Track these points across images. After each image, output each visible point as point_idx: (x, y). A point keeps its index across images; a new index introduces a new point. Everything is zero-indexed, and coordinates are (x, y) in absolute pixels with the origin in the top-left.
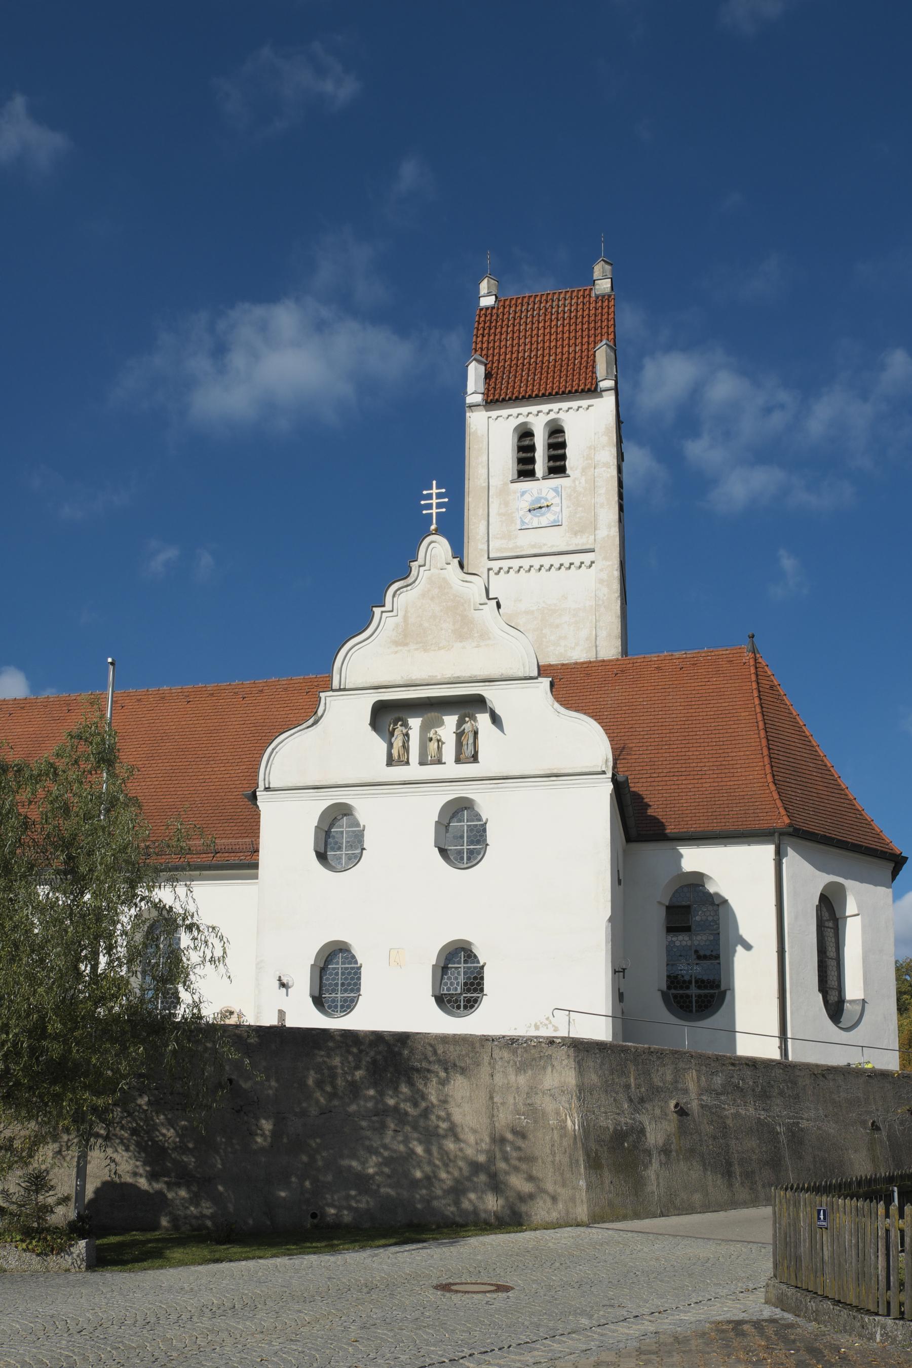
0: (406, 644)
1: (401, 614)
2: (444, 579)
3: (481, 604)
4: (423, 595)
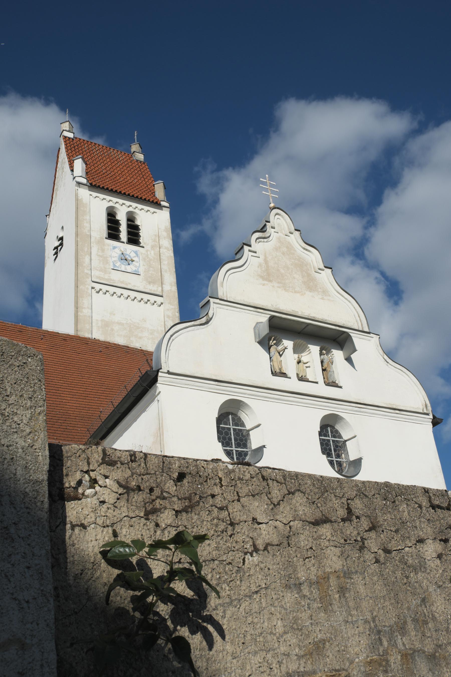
0: (270, 281)
1: (262, 257)
2: (289, 243)
3: (319, 269)
4: (276, 249)
